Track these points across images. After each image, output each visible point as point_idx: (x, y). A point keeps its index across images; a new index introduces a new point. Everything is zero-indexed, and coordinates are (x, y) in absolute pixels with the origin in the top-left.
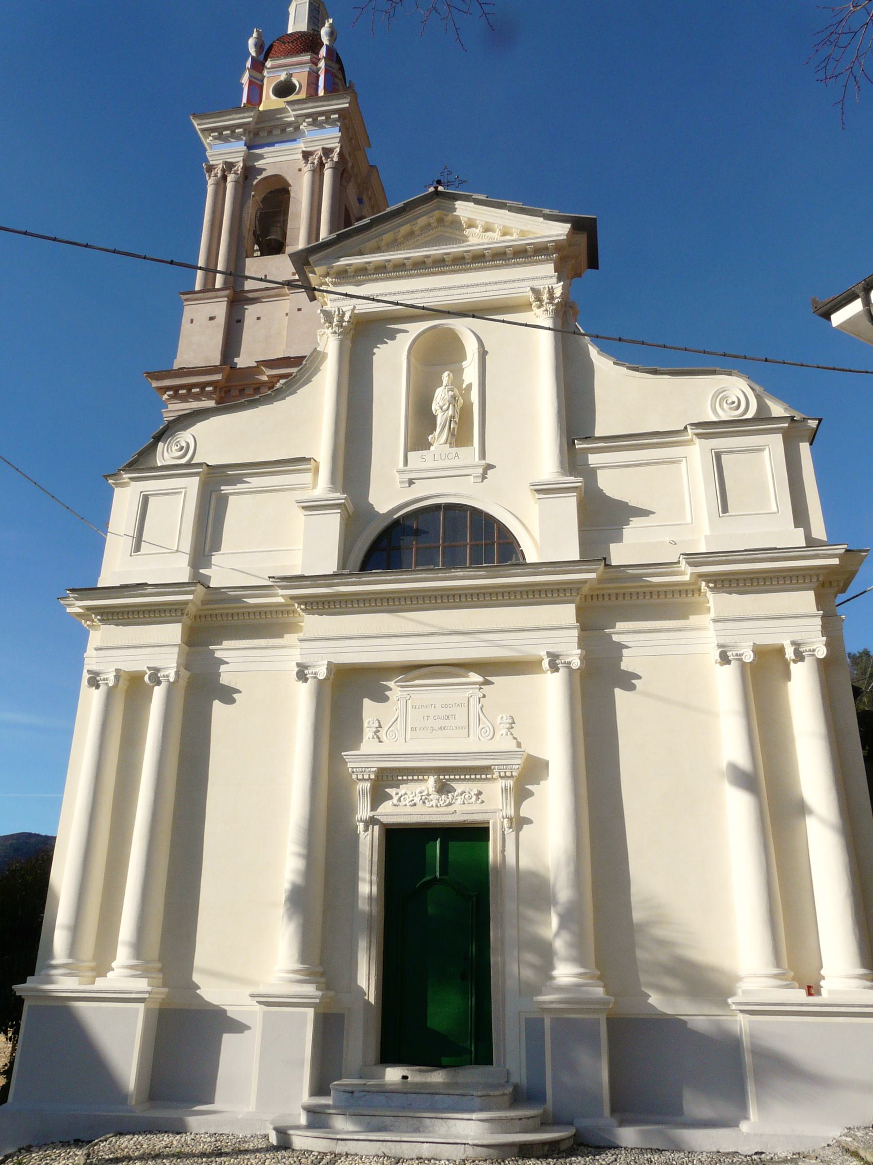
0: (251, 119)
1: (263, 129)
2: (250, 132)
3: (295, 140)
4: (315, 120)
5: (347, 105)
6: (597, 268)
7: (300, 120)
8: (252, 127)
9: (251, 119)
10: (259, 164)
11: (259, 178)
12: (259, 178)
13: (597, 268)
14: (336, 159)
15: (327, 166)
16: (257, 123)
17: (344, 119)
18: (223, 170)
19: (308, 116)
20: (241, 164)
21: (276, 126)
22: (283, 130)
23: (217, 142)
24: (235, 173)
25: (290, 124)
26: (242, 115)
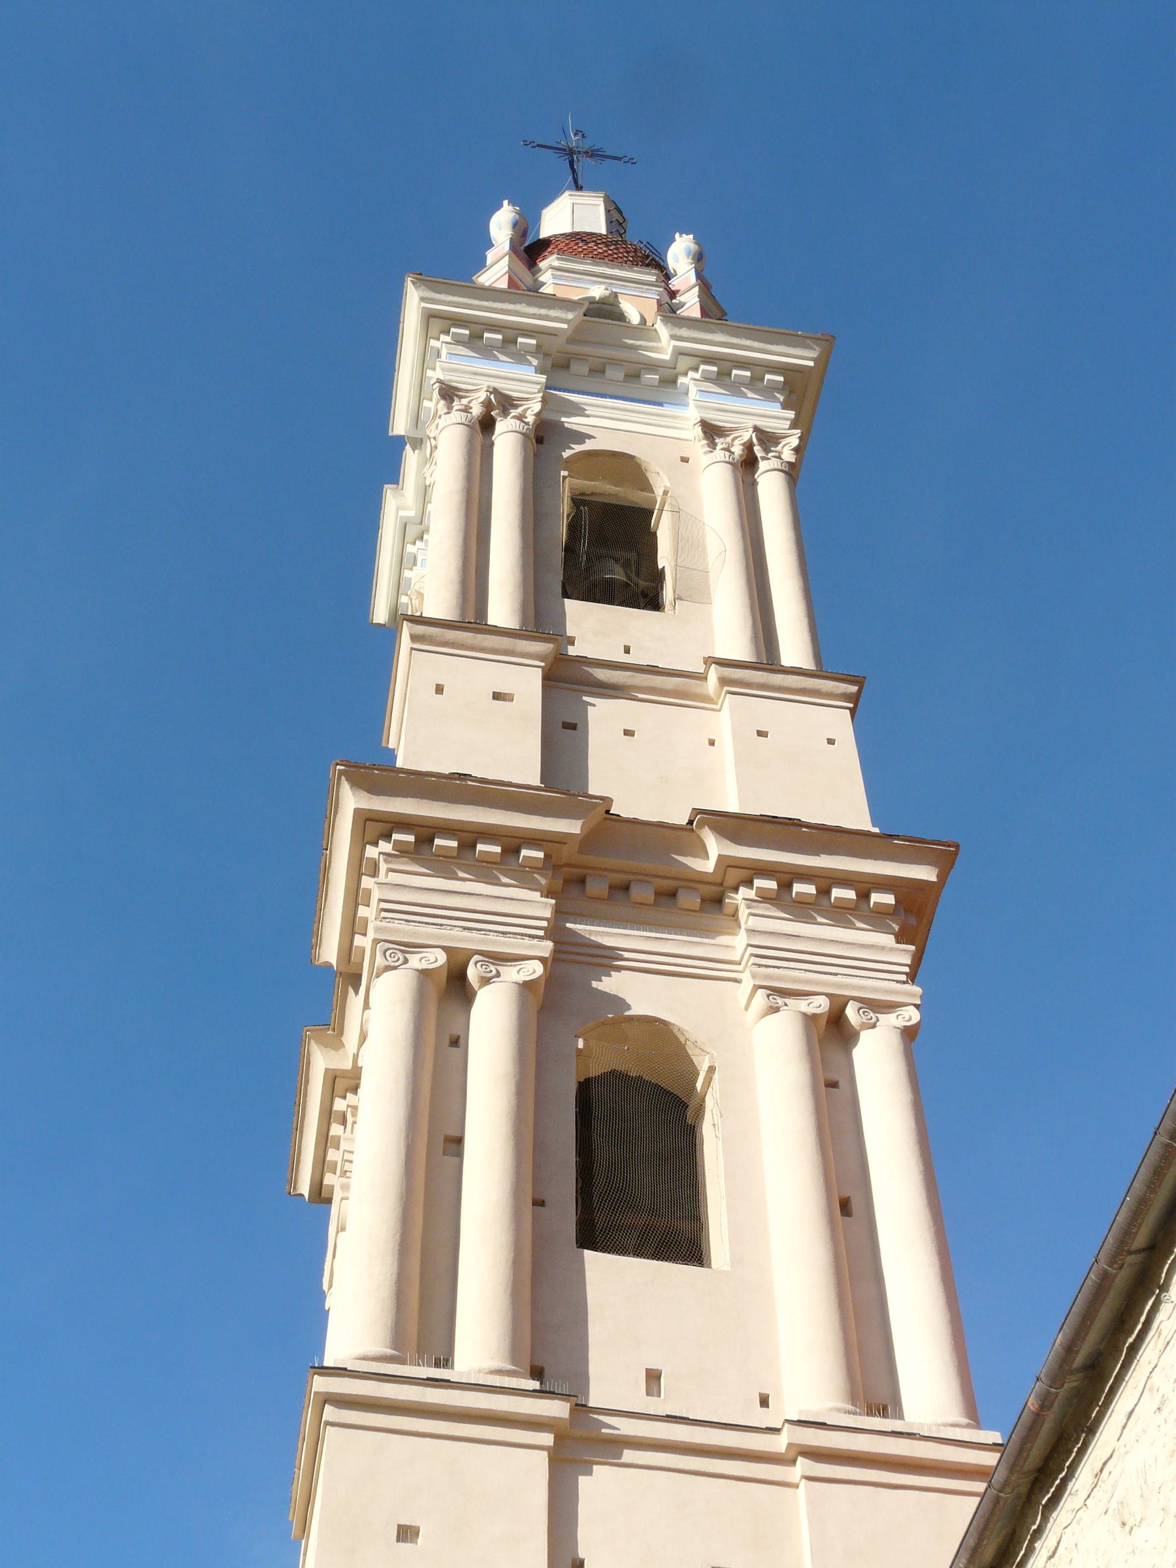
0: (565, 326)
1: (581, 358)
2: (546, 355)
3: (660, 404)
4: (723, 373)
5: (811, 364)
6: (399, 1526)
7: (683, 363)
8: (559, 344)
9: (565, 326)
10: (572, 422)
11: (578, 448)
12: (578, 448)
13: (399, 1526)
14: (788, 456)
15: (763, 465)
16: (571, 340)
17: (791, 392)
18: (487, 405)
19: (709, 359)
20: (537, 407)
21: (617, 363)
22: (633, 376)
23: (461, 350)
24: (520, 418)
25: (653, 366)
26: (543, 311)
